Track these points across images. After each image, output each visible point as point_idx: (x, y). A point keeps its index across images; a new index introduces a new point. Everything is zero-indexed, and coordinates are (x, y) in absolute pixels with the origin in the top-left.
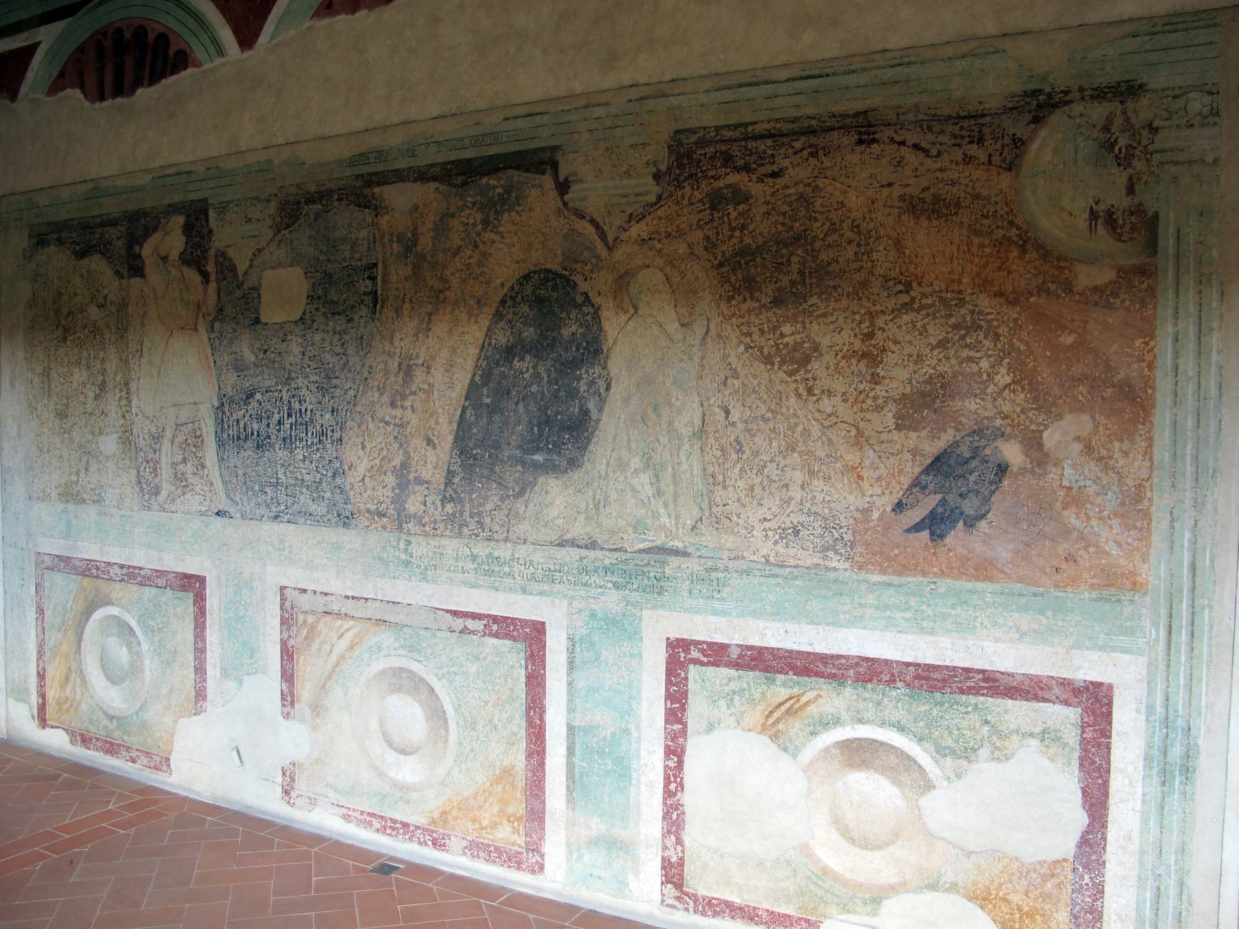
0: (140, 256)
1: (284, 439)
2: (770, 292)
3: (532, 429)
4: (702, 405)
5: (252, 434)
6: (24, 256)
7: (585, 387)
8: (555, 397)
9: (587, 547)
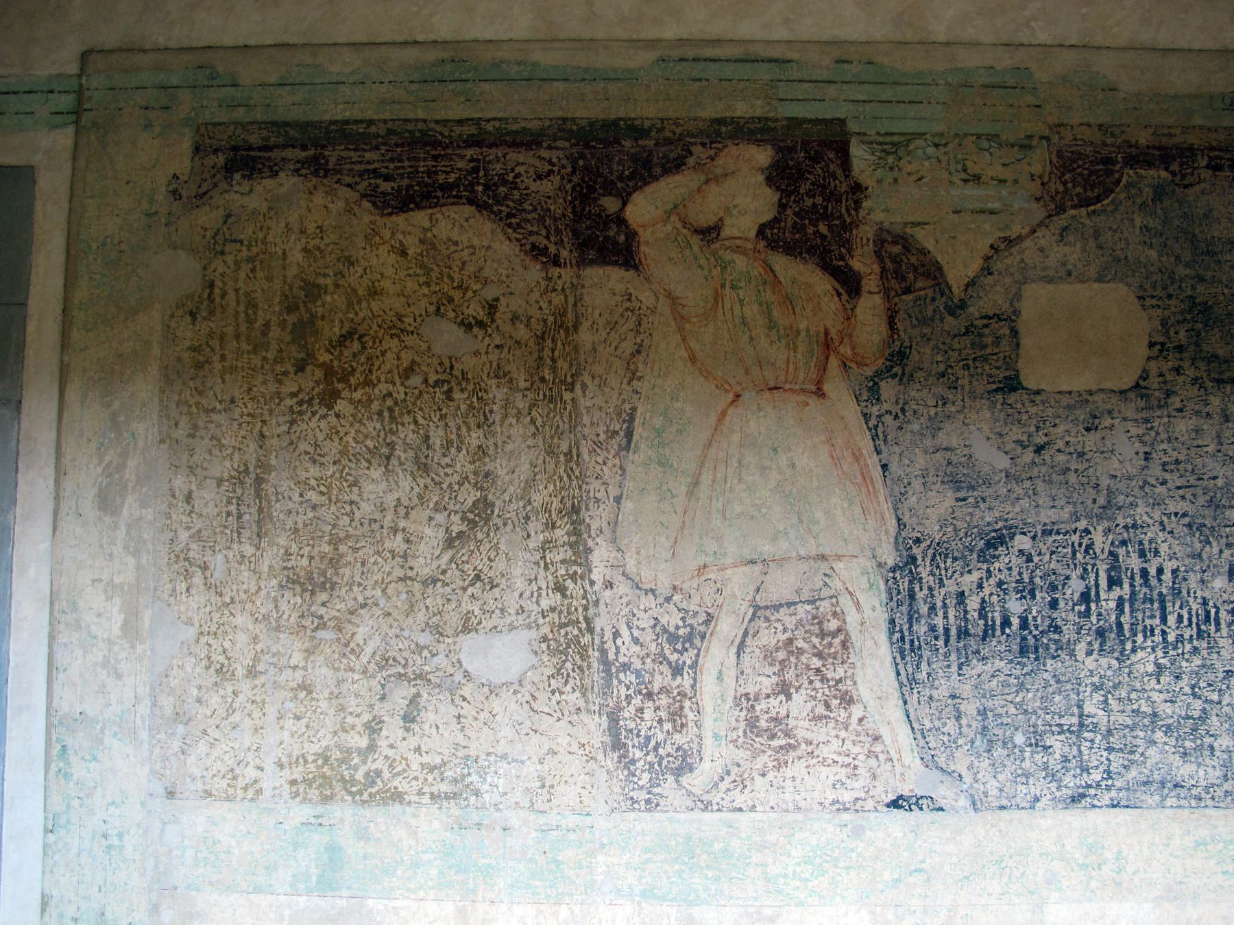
0: (621, 221)
1: (1101, 633)
5: (1006, 622)
6: (177, 195)
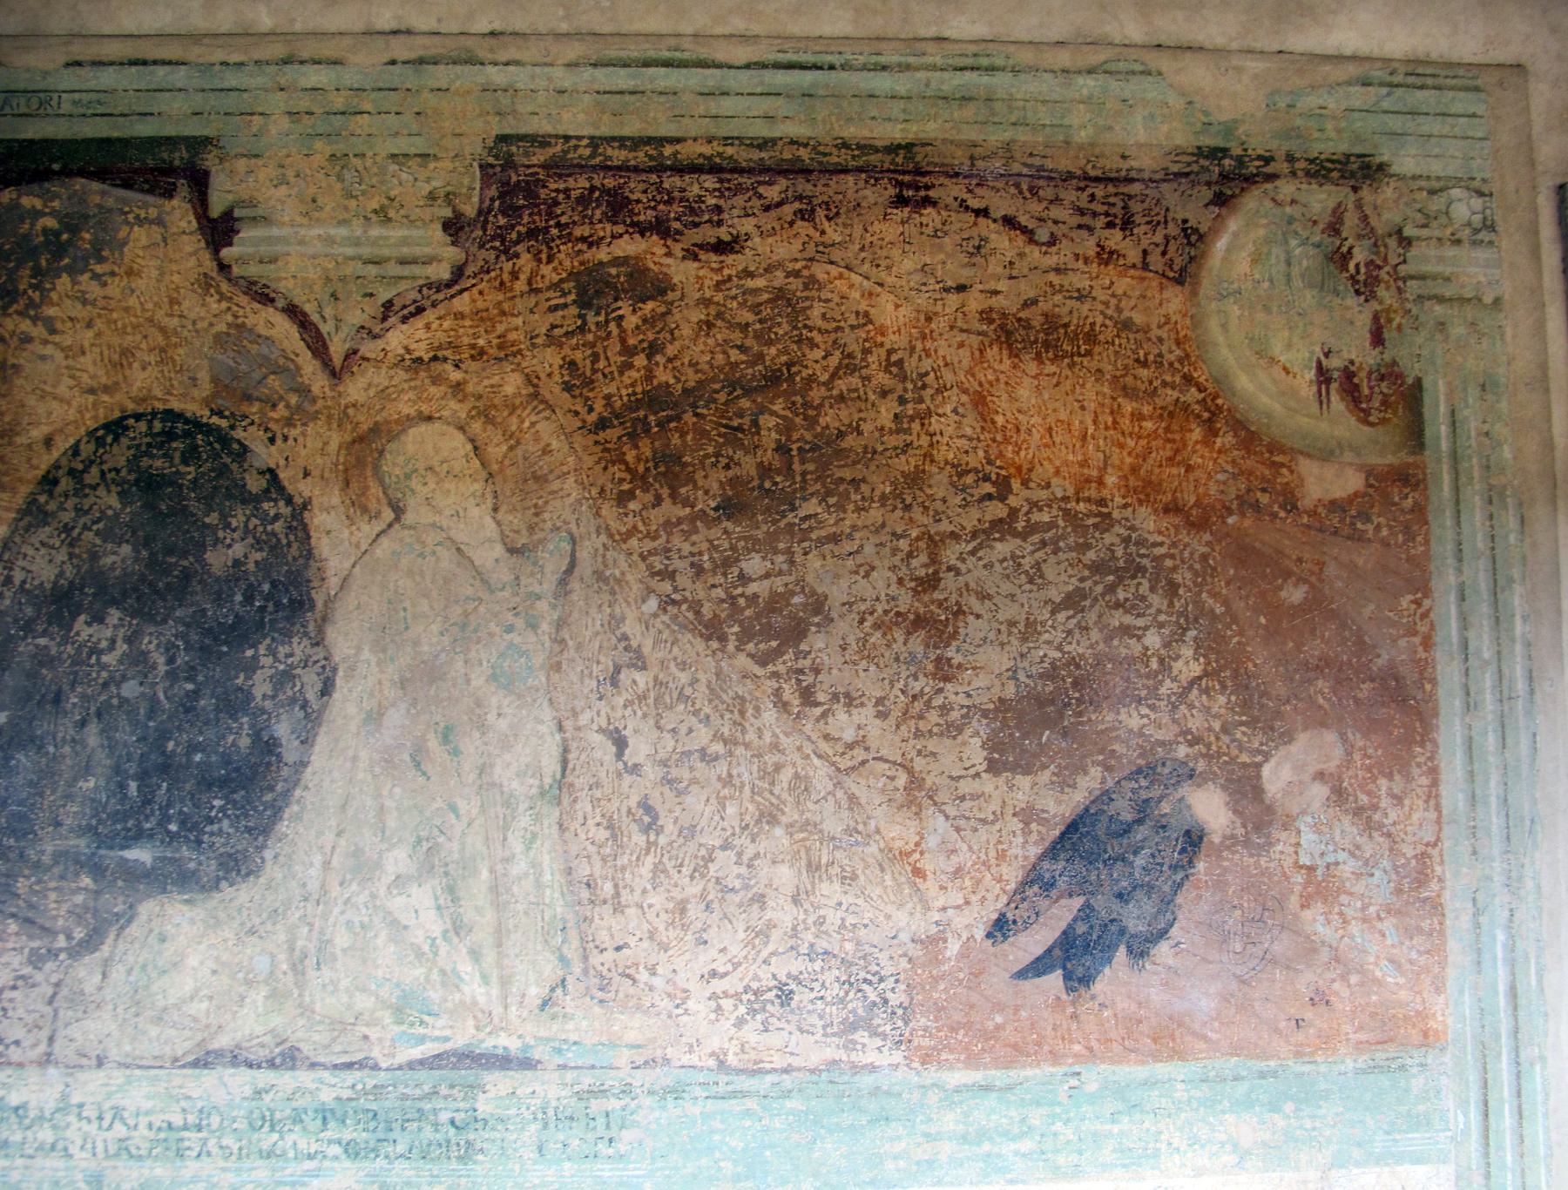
2: (715, 486)
3: (122, 786)
4: (561, 728)
7: (267, 688)
8: (187, 711)
9: (272, 1064)
